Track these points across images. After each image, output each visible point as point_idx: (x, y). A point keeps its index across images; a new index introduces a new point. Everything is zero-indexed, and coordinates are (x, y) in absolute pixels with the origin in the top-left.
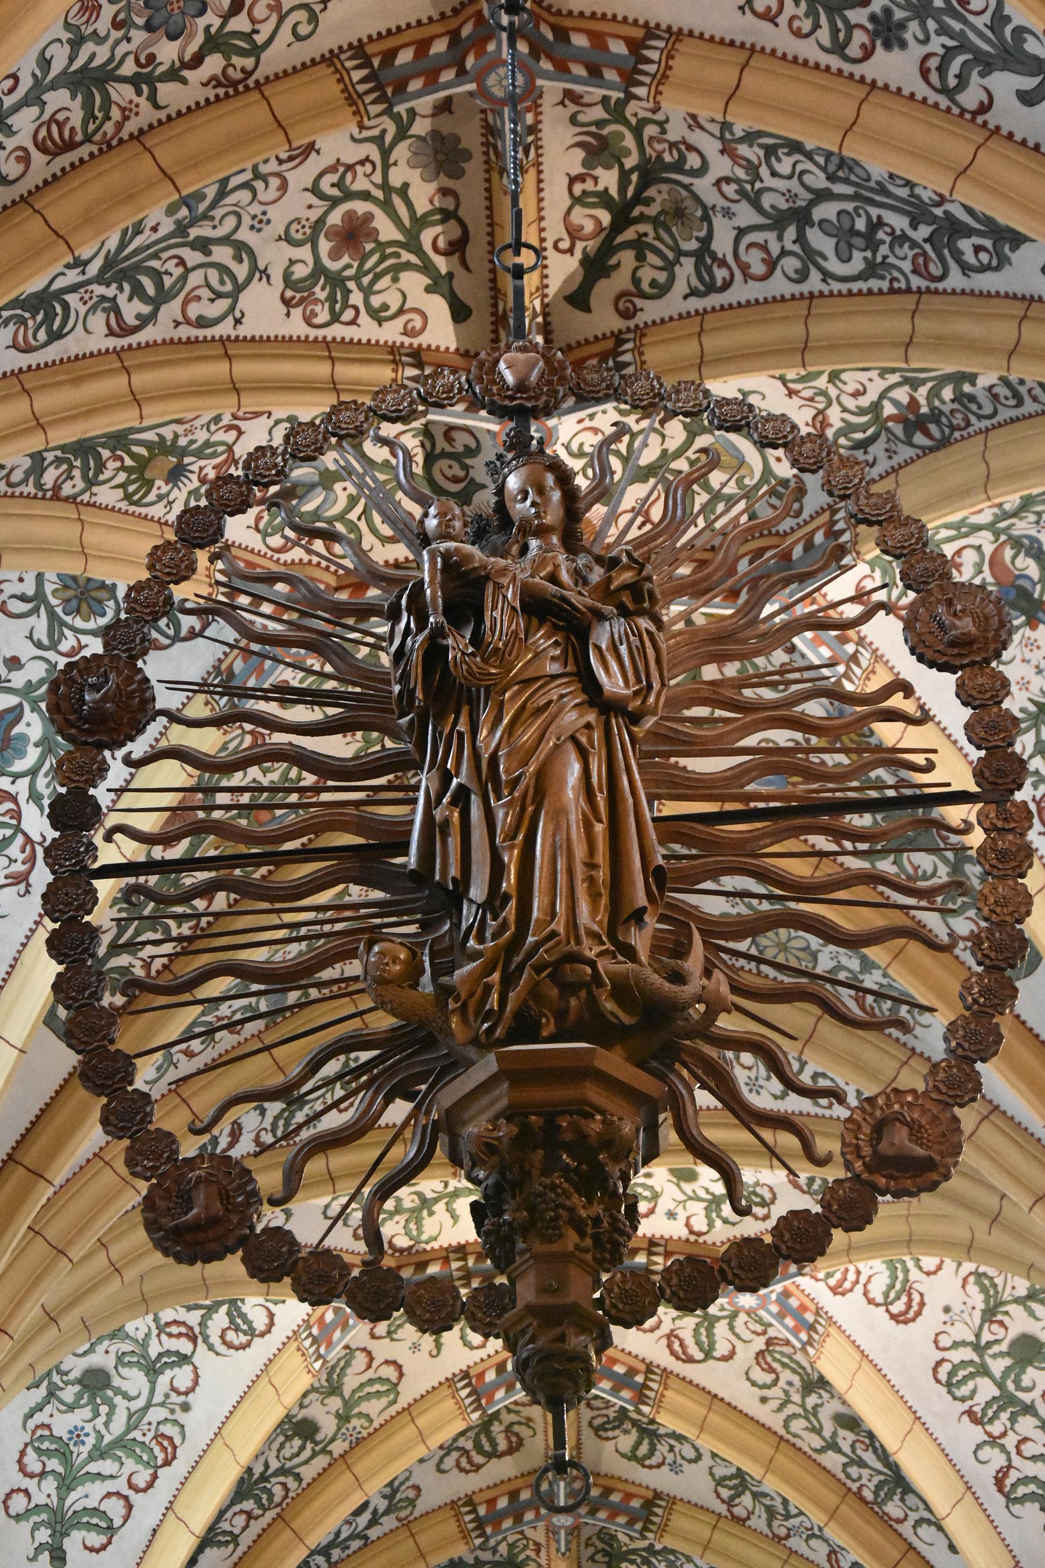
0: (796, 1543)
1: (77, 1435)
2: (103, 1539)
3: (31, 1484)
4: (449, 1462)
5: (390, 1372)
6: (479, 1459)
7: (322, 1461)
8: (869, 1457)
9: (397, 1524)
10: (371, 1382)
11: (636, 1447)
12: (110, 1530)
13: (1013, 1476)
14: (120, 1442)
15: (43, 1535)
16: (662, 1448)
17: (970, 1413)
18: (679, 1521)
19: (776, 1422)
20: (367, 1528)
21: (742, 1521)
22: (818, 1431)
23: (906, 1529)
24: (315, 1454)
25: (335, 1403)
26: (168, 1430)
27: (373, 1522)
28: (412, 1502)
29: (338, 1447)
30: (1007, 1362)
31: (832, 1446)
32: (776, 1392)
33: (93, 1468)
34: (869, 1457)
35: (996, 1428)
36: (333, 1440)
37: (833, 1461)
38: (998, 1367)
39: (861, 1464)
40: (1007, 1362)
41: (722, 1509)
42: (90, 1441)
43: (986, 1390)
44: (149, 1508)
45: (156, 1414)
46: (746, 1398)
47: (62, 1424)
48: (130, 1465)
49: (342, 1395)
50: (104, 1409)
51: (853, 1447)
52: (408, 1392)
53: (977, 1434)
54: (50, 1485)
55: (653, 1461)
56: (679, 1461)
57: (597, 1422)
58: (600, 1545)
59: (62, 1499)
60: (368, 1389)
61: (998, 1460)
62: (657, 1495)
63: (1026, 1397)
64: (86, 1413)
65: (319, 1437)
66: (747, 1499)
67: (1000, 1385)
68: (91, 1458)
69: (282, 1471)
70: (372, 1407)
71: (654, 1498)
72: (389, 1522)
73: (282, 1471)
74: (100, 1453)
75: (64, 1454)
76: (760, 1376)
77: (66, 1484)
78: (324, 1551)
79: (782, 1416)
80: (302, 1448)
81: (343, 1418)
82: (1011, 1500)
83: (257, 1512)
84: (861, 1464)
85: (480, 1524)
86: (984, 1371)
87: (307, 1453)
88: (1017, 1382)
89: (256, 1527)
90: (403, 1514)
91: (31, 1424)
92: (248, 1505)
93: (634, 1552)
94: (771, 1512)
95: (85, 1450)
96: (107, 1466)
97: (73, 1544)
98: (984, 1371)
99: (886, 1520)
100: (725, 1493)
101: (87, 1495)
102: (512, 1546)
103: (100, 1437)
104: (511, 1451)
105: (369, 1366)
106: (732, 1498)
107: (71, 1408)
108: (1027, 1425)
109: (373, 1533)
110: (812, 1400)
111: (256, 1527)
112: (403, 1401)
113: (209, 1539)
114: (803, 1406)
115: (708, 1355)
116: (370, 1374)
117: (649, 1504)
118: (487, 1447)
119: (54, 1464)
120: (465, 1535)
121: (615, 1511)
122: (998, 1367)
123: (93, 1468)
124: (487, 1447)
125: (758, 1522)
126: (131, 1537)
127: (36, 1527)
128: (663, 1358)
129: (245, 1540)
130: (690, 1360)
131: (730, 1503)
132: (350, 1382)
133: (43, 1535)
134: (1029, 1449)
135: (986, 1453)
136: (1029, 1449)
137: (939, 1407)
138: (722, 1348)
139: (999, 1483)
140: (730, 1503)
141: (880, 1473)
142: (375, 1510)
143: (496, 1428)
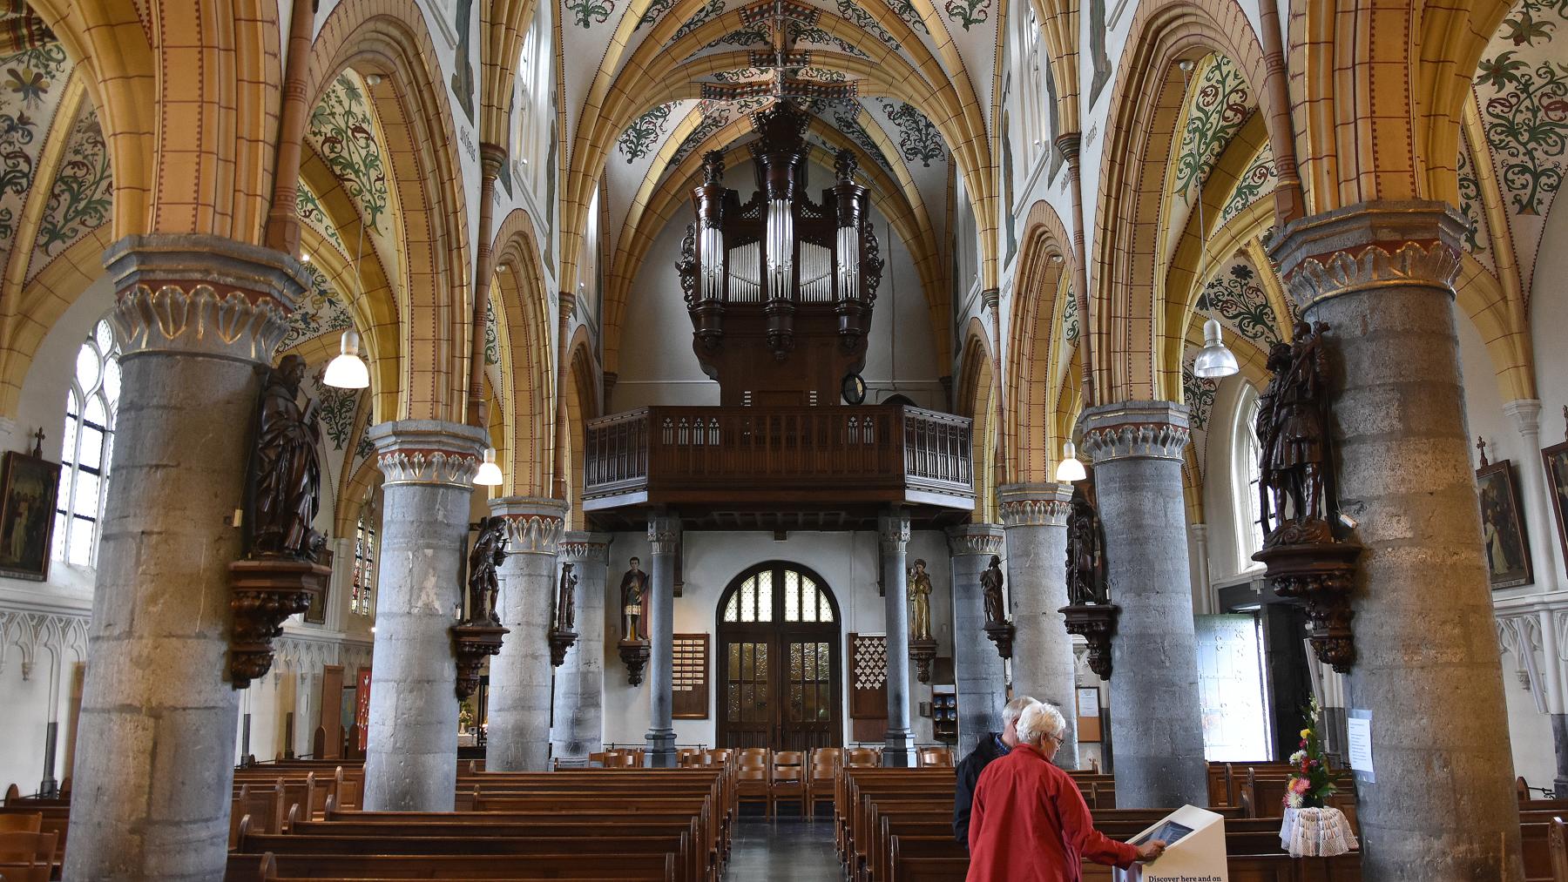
0: (868, 29)
12: (606, 14)
15: (581, 15)
23: (910, 25)
72: (713, 16)
78: (688, 26)
82: (951, 15)
85: (748, 17)
89: (662, 15)
97: (592, 19)
99: (903, 20)
111: (662, 15)
113: (643, 19)
117: (812, 12)
121: (799, 14)
125: (854, 20)
129: (658, 20)
133: (581, 15)
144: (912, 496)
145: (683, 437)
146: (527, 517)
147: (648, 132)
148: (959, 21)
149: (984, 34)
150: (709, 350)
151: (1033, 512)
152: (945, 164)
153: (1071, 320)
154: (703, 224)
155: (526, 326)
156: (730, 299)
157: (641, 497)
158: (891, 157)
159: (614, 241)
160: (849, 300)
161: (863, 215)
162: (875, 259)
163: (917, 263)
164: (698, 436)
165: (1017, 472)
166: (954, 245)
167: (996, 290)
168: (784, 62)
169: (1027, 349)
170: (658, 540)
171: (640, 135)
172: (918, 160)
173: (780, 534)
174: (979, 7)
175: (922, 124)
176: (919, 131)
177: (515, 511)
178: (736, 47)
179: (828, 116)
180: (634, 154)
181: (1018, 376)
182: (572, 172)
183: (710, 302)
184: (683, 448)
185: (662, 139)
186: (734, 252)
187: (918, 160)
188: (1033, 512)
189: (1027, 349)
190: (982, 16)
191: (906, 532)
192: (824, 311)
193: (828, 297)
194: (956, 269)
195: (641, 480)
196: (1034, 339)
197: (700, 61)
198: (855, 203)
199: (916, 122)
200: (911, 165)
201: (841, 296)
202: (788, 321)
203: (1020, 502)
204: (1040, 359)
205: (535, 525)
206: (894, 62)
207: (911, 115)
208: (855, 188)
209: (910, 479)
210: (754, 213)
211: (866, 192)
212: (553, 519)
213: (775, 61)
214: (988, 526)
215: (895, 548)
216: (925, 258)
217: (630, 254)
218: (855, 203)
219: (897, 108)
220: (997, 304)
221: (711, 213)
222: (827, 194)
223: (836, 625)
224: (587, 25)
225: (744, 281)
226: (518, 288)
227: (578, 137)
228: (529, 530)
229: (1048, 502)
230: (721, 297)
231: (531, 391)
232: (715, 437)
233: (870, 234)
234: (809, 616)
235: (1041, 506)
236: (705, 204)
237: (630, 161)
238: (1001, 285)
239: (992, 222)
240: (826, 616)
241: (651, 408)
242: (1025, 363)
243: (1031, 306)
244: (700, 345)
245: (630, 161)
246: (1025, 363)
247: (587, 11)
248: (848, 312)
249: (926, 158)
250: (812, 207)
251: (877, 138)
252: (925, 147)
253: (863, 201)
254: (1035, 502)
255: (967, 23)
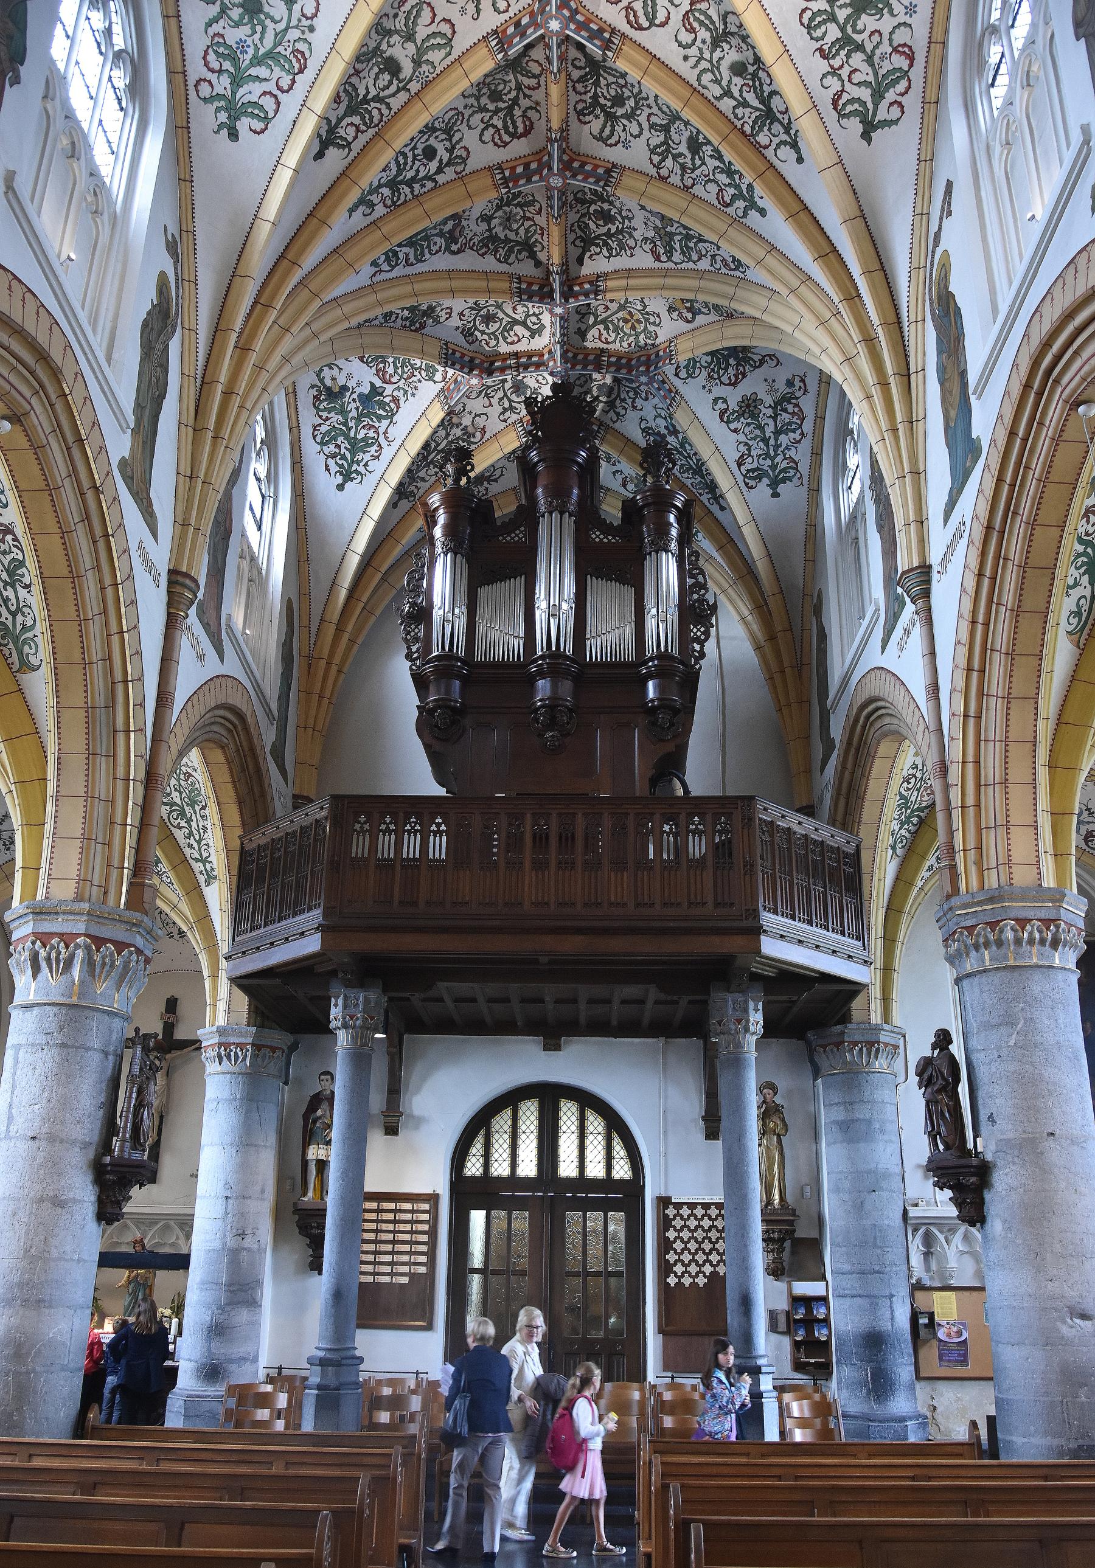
0: (698, 190)
1: (242, 45)
2: (261, 125)
3: (213, 77)
4: (488, 134)
5: (445, 28)
6: (506, 138)
7: (403, 97)
8: (751, 98)
9: (454, 176)
10: (434, 35)
11: (602, 131)
12: (266, 119)
13: (845, 97)
14: (269, 54)
15: (223, 117)
16: (619, 129)
17: (820, 50)
18: (627, 180)
19: (691, 76)
20: (436, 173)
21: (663, 179)
22: (717, 82)
23: (769, 153)
24: (399, 90)
25: (411, 48)
26: (302, 46)
27: (440, 170)
28: (464, 161)
29: (414, 87)
30: (849, 11)
31: (728, 93)
32: (693, 51)
33: (253, 71)
34: (751, 98)
35: (836, 63)
36: (410, 80)
37: (727, 105)
38: (842, 14)
39: (745, 104)
40: (849, 11)
41: (653, 171)
42: (251, 51)
43: (833, 32)
44: (290, 103)
45: (293, 34)
46: (672, 55)
47: (233, 36)
48: (277, 72)
49: (415, 42)
50: (259, 28)
51: (741, 91)
52: (458, 49)
53: (823, 66)
54: (225, 80)
55: (612, 141)
56: (629, 138)
57: (580, 106)
58: (580, 233)
59: (234, 93)
60: (432, 41)
61: (835, 84)
62: (614, 166)
63: (858, 38)
64: (247, 29)
65: (402, 76)
66: (669, 162)
67: (843, 30)
68: (252, 65)
69: (377, 99)
70: (435, 56)
71: (612, 168)
72: (449, 173)
73: (377, 99)
74: (257, 61)
75: (235, 61)
76: (686, 37)
77: (237, 81)
78: (410, 183)
79: (697, 71)
80: (391, 83)
81: (417, 63)
82: (842, 115)
83: (363, 127)
84: (745, 104)
85: (506, 181)
86: (833, 18)
87: (393, 88)
88: (854, 26)
89: (363, 139)
90: (459, 168)
91: (211, 31)
92: (356, 120)
93: (598, 237)
94: (683, 167)
95: (248, 57)
96: (262, 72)
97: (243, 125)
98: (833, 18)
99: (758, 148)
100: (656, 159)
101: (250, 92)
102: (527, 231)
103: (257, 49)
104: (526, 134)
105: (433, 22)
106: (660, 163)
107: (237, 24)
108: (857, 59)
109: (441, 179)
110: (717, 54)
111: (363, 139)
112: (456, 54)
114: (711, 62)
115: (652, 24)
116: (433, 28)
117: (608, 171)
118: (511, 130)
119: (227, 65)
120: (496, 186)
122: (842, 14)
123: (253, 71)
124: (511, 130)
125: (675, 179)
126: (280, 125)
127: (218, 110)
128: (623, 26)
129: (356, 147)
130: (640, 28)
131: (658, 167)
132: (421, 33)
134: (857, 78)
135: (830, 80)
136: (857, 78)
137: (801, 43)
138: (661, 17)
139: (835, 103)
140: (658, 167)
141: (757, 109)
142: (441, 161)
143: (517, 112)
144: (770, 947)
145: (386, 847)
146: (67, 939)
147: (367, 442)
148: (855, 126)
149: (898, 145)
150: (439, 730)
151: (1018, 941)
152: (804, 490)
153: (1076, 593)
154: (439, 549)
155: (75, 577)
156: (478, 658)
157: (312, 944)
158: (724, 482)
159: (317, 609)
160: (663, 656)
161: (685, 539)
162: (702, 600)
163: (758, 648)
164: (411, 847)
165: (981, 871)
166: (818, 609)
167: (925, 571)
168: (566, 296)
169: (1001, 636)
170: (345, 1026)
171: (356, 446)
172: (763, 488)
173: (552, 1044)
174: (890, 96)
175: (769, 430)
176: (765, 441)
177: (47, 927)
178: (490, 263)
179: (631, 427)
180: (347, 477)
181: (981, 694)
182: (205, 384)
183: (448, 657)
184: (386, 866)
185: (387, 452)
186: (484, 592)
187: (763, 488)
188: (1018, 941)
189: (1001, 636)
190: (895, 112)
191: (756, 1018)
192: (625, 675)
193: (630, 656)
194: (823, 636)
195: (315, 916)
196: (1017, 612)
197: (433, 274)
198: (672, 518)
199: (761, 427)
200: (751, 495)
201: (650, 650)
202: (566, 687)
203: (993, 925)
204: (1028, 655)
205: (80, 954)
206: (741, 239)
207: (754, 416)
208: (671, 495)
209: (768, 919)
210: (519, 535)
211: (688, 504)
212: (120, 946)
213: (550, 295)
214: (878, 1029)
215: (739, 1045)
216: (772, 638)
217: (340, 629)
218: (672, 518)
219: (733, 405)
220: (926, 594)
221: (451, 531)
222: (629, 507)
223: (633, 1189)
224: (234, 135)
225: (502, 639)
226: (51, 489)
227: (218, 330)
228: (69, 963)
229: (1047, 922)
230: (462, 653)
231: (90, 708)
232: (439, 848)
233: (695, 565)
234: (595, 1170)
235: (1033, 930)
236: (442, 518)
237: (340, 487)
238: (935, 558)
239: (914, 460)
240: (622, 1170)
241: (335, 798)
242: (997, 665)
243: (1015, 548)
244: (427, 725)
245: (340, 487)
246: (997, 665)
247: (235, 111)
248: (660, 674)
249: (774, 484)
250: (606, 528)
251: (705, 451)
252: (774, 467)
253: (685, 517)
254: (1022, 922)
255: (869, 129)
